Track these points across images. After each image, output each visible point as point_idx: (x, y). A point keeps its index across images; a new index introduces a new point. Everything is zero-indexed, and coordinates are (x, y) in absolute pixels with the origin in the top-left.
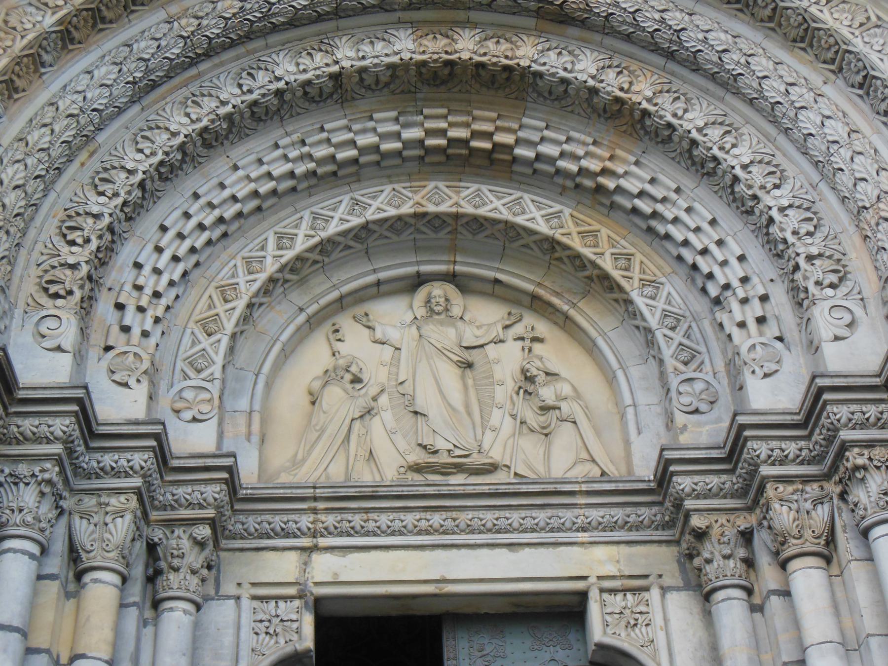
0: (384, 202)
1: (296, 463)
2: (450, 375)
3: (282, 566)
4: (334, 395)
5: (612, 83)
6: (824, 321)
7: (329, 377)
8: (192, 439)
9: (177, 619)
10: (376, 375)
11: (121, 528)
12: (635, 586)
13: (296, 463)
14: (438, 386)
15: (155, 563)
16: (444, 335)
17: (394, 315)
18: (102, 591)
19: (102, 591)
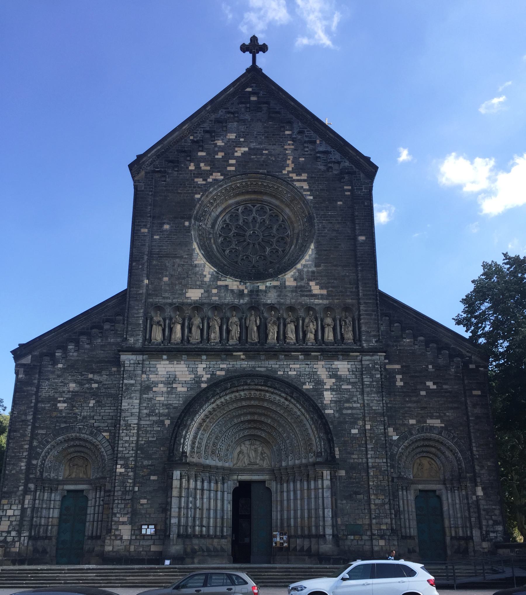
0: (246, 433)
1: (237, 463)
2: (253, 453)
3: (235, 477)
4: (241, 455)
5: (272, 424)
6: (290, 458)
7: (240, 452)
8: (227, 465)
9: (226, 485)
10: (245, 452)
11: (221, 478)
12: (270, 480)
13: (237, 463)
14: (252, 454)
15: (223, 479)
16: (253, 447)
17: (247, 443)
18: (219, 485)
19: (219, 485)
